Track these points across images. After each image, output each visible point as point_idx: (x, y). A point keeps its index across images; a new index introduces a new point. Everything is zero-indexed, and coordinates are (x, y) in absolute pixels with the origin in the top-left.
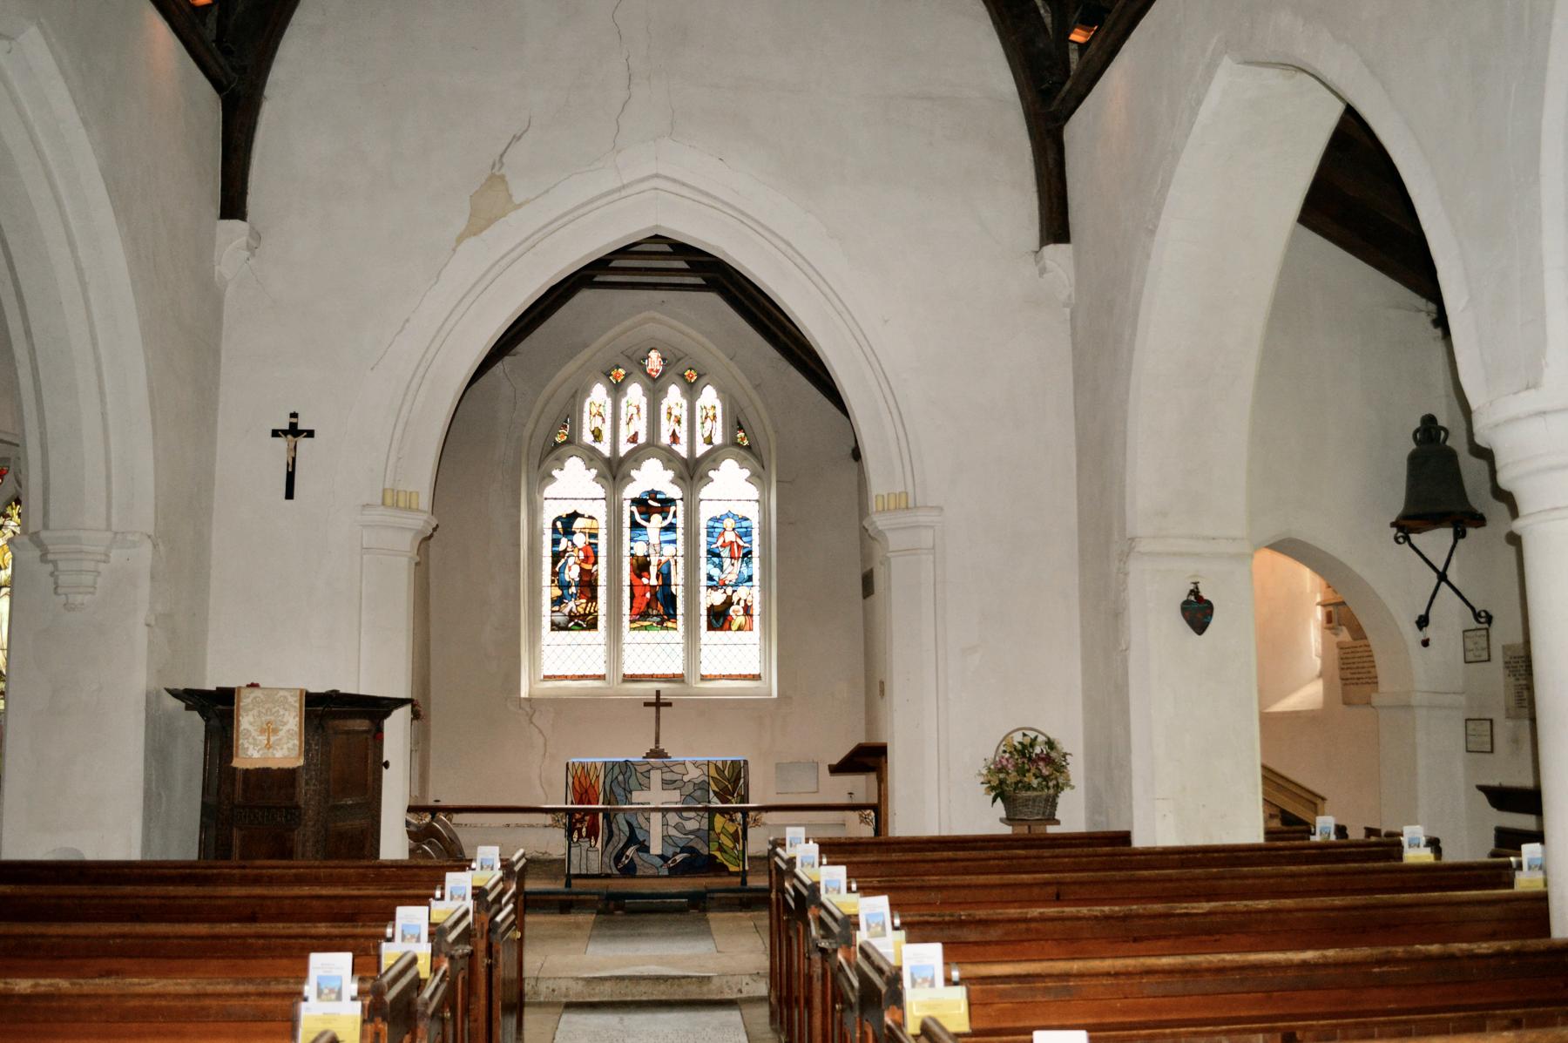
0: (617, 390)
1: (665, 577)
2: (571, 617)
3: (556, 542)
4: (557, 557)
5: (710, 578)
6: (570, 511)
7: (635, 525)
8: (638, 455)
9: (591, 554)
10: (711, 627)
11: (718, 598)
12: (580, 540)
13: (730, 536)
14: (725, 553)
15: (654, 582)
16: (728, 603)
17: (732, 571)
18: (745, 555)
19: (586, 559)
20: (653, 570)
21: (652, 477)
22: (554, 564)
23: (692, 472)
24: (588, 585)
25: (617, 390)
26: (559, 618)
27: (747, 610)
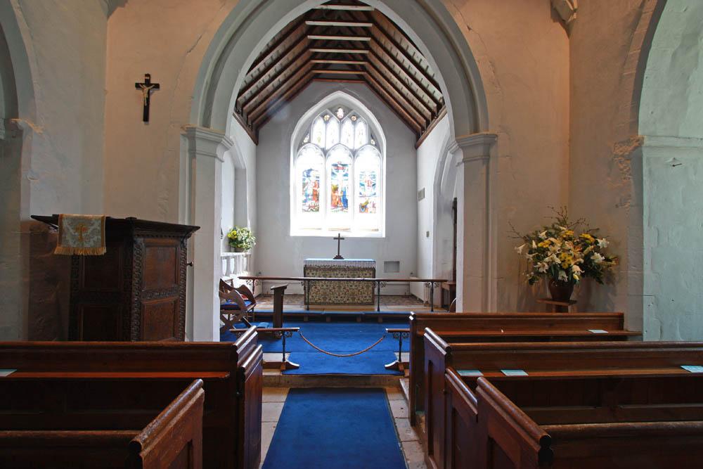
0: (326, 122)
1: (344, 193)
2: (310, 207)
3: (304, 179)
4: (304, 185)
5: (361, 194)
6: (309, 168)
7: (333, 174)
8: (333, 148)
9: (317, 185)
10: (360, 211)
11: (363, 201)
12: (313, 179)
13: (368, 178)
14: (366, 184)
15: (340, 195)
16: (367, 203)
17: (369, 191)
18: (374, 185)
19: (315, 186)
20: (340, 190)
21: (340, 156)
22: (304, 187)
23: (354, 153)
24: (316, 196)
25: (326, 122)
26: (306, 208)
27: (374, 206)
